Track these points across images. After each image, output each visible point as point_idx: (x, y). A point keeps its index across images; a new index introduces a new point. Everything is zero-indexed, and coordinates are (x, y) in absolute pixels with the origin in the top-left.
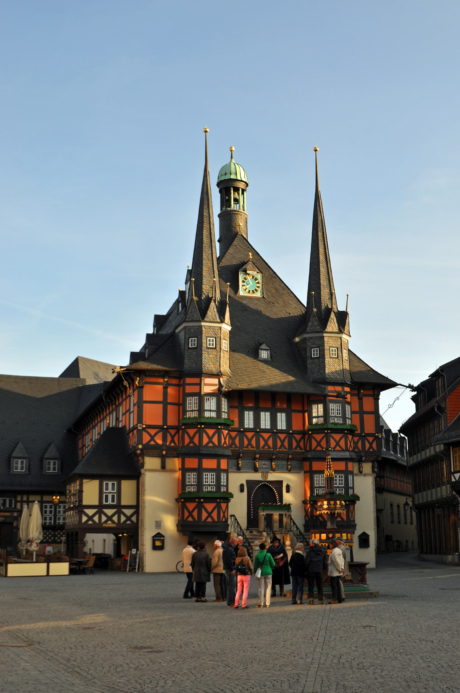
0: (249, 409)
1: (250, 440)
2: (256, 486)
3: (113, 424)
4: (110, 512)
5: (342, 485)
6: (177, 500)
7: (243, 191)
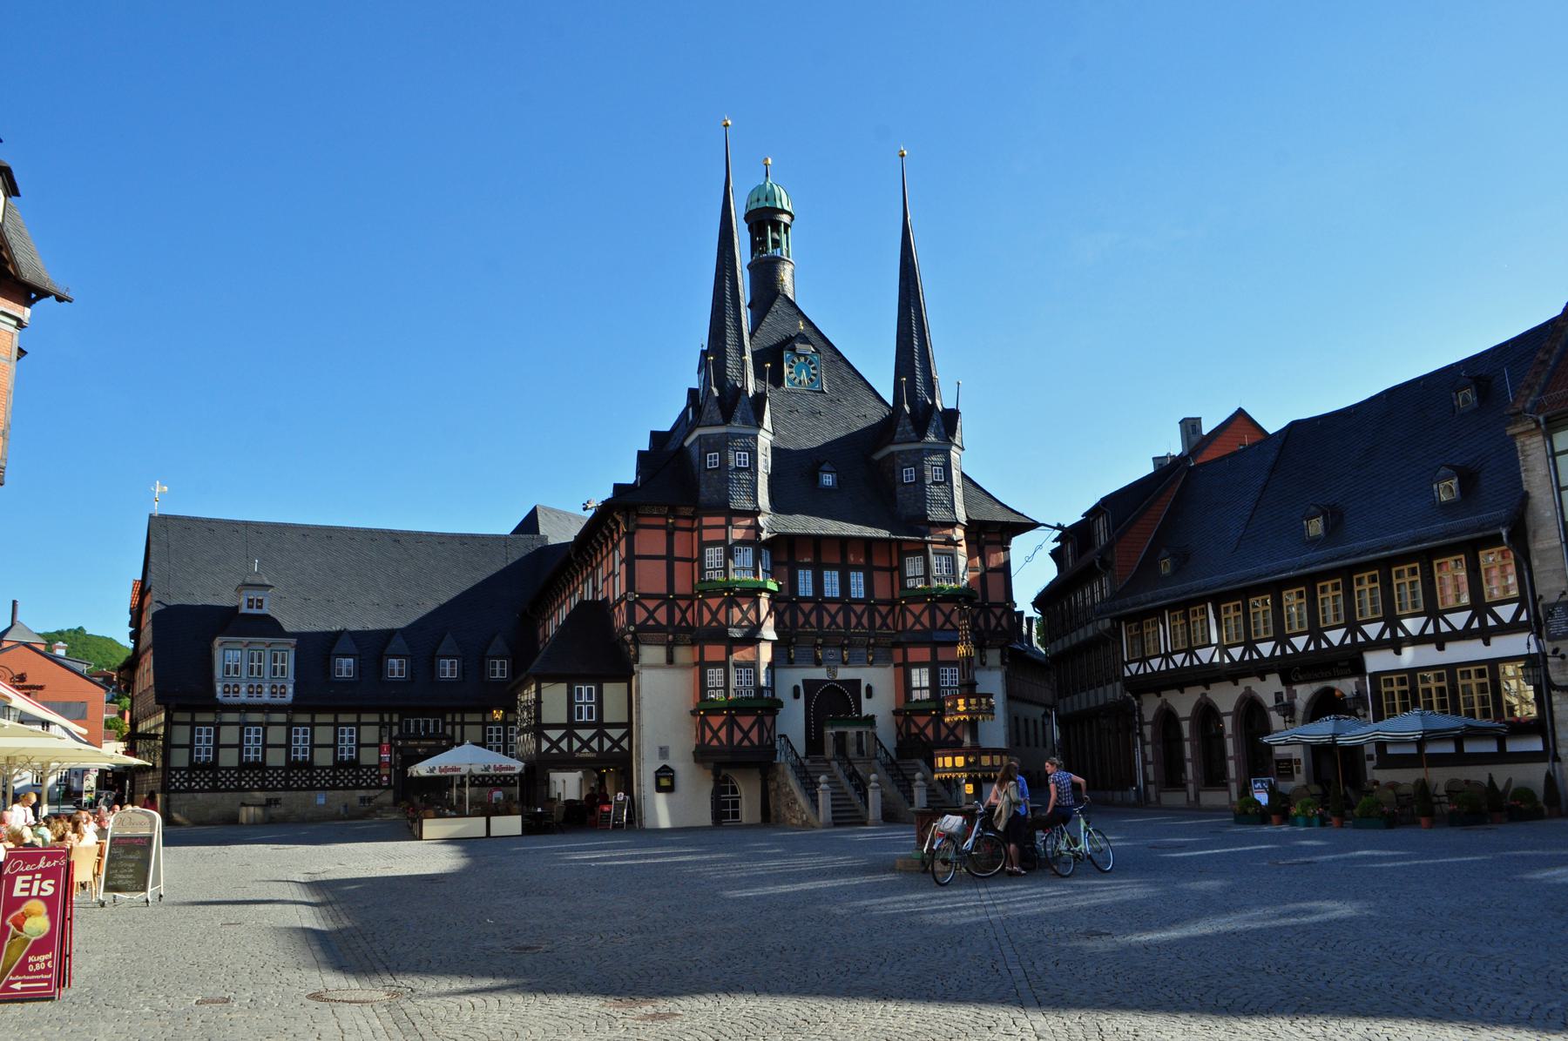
0: (805, 566)
1: (807, 616)
3: (589, 596)
4: (585, 734)
6: (694, 713)
7: (787, 226)
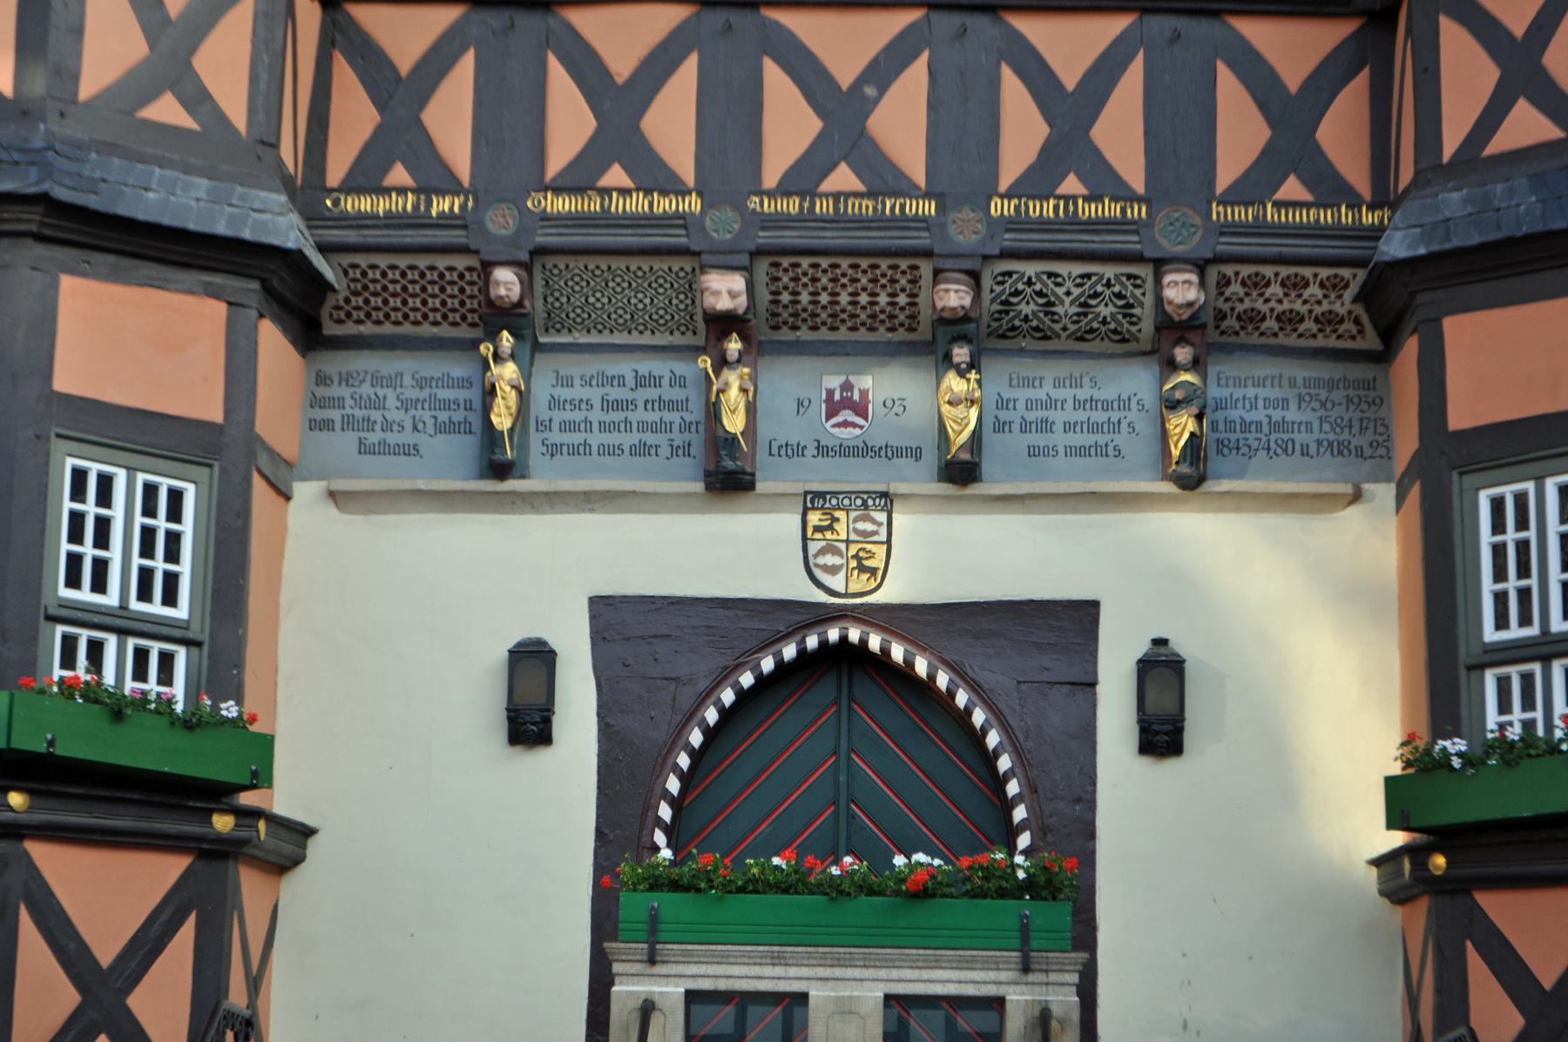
2: (727, 674)
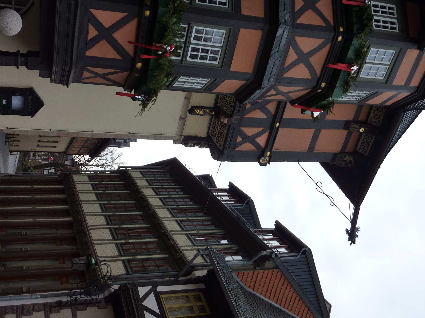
5: (192, 56)
